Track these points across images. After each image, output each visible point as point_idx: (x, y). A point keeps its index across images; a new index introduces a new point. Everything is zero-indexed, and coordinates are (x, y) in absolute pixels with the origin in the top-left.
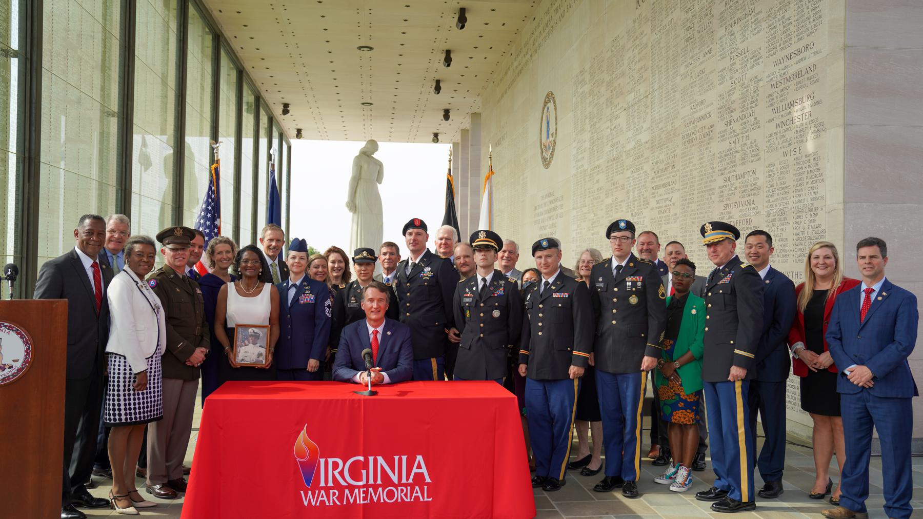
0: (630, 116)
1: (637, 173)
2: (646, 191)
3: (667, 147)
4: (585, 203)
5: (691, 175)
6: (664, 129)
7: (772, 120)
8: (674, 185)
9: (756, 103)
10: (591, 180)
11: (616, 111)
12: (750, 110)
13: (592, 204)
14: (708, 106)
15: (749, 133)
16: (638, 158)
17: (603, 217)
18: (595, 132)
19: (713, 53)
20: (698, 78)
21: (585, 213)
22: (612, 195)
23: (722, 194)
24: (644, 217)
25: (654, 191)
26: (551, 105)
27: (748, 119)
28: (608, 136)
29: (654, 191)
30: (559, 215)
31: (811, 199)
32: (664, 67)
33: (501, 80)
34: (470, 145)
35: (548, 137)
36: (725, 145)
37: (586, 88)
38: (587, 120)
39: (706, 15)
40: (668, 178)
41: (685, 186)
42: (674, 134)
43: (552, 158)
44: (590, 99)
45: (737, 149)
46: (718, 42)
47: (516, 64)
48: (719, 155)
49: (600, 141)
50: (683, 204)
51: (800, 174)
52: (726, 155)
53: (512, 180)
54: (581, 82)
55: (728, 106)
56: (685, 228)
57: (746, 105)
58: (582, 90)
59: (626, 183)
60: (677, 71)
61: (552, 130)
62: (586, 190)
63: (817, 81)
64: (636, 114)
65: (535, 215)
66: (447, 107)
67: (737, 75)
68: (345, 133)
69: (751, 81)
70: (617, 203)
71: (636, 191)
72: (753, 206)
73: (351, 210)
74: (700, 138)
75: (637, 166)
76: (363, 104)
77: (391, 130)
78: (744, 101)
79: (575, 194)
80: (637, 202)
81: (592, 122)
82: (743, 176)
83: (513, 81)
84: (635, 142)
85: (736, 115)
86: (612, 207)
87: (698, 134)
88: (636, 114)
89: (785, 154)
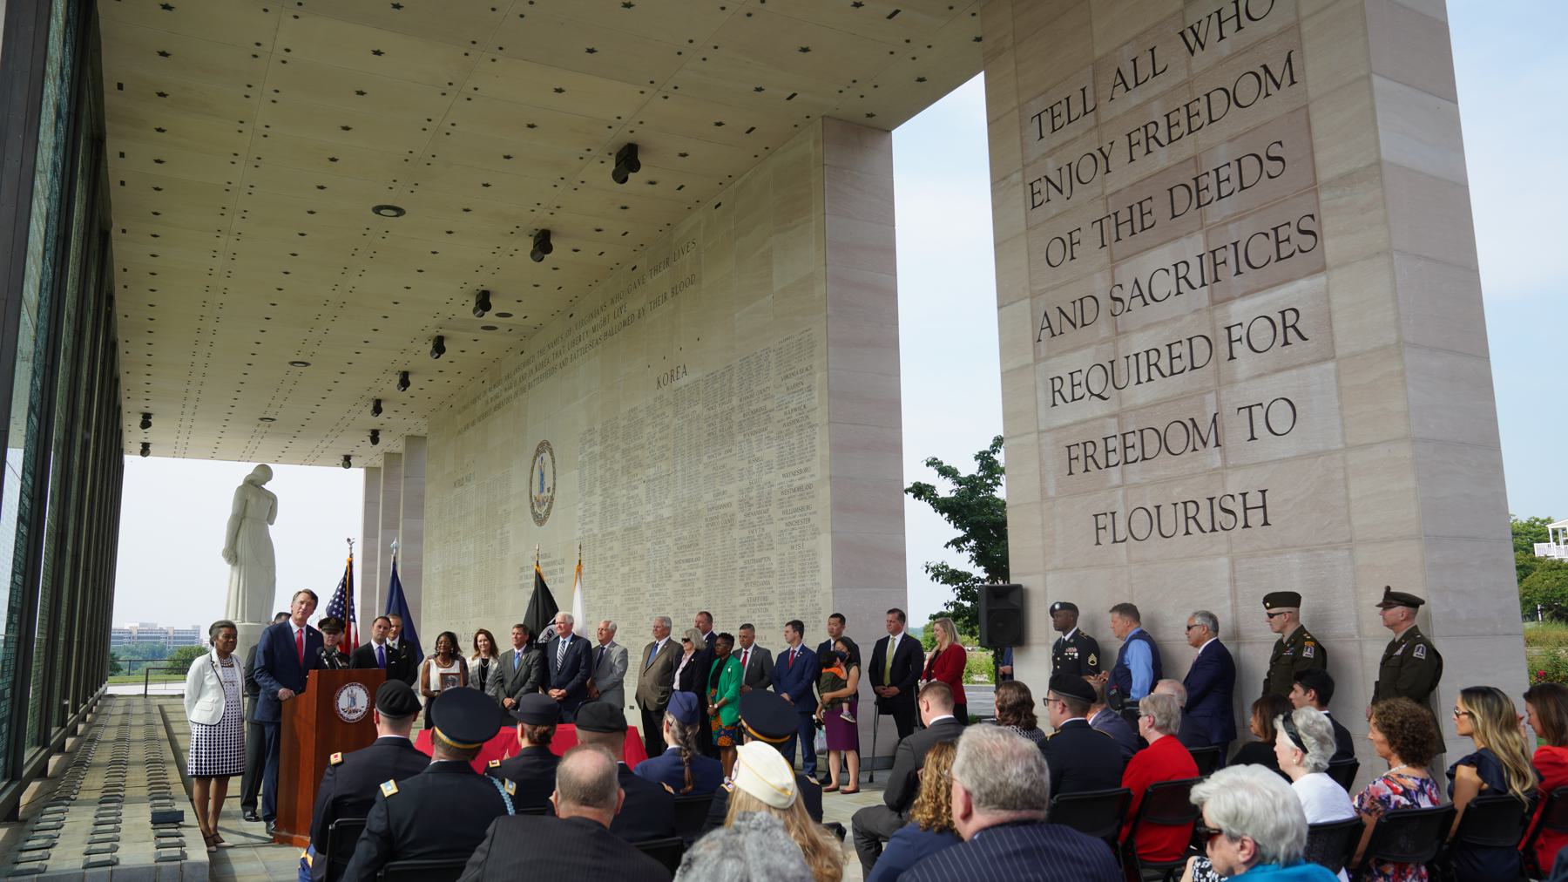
7: (782, 519)
12: (765, 508)
14: (729, 497)
16: (660, 531)
18: (608, 497)
19: (733, 452)
21: (596, 580)
26: (546, 456)
31: (812, 584)
33: (465, 408)
34: (403, 476)
35: (542, 491)
36: (745, 533)
37: (597, 449)
38: (598, 484)
39: (727, 418)
44: (602, 462)
47: (490, 395)
51: (803, 564)
53: (484, 533)
54: (589, 441)
58: (592, 449)
61: (548, 483)
63: (813, 496)
65: (521, 577)
66: (377, 427)
67: (754, 477)
68: (215, 450)
76: (262, 419)
82: (760, 560)
83: (485, 415)
85: (754, 509)
87: (720, 520)
88: (657, 489)
89: (792, 548)
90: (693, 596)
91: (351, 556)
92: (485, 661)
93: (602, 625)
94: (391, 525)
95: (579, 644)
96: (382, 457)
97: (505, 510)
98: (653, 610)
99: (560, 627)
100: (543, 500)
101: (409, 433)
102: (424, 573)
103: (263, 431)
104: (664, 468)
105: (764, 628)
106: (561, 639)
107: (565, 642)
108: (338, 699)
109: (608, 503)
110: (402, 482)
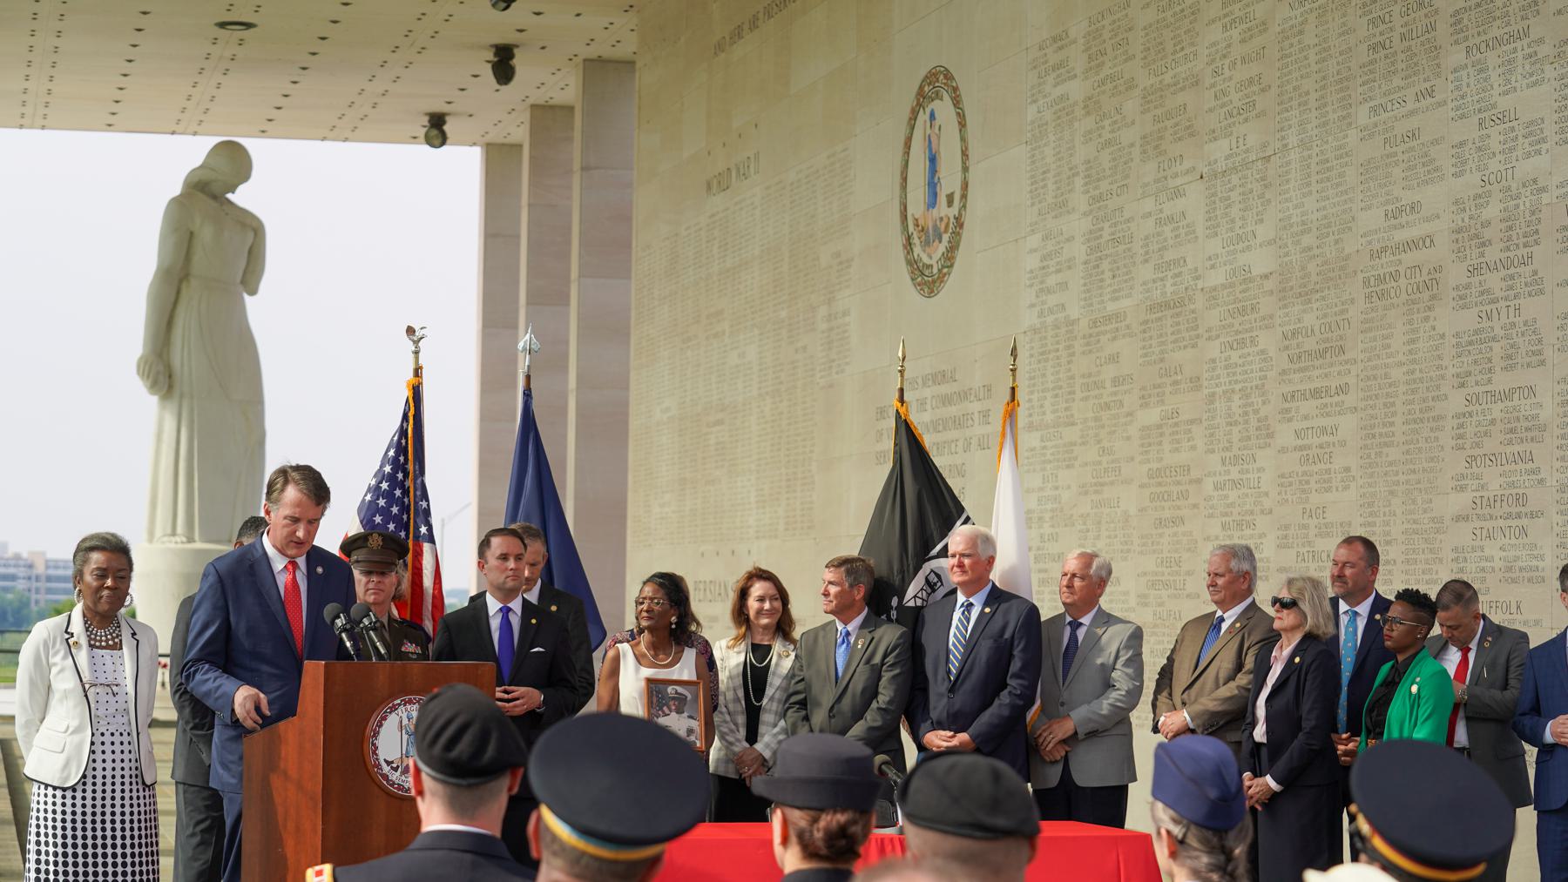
0: (1217, 199)
1: (1240, 352)
2: (1264, 403)
3: (1323, 298)
4: (1072, 416)
5: (1386, 376)
6: (1316, 252)
8: (1343, 397)
9: (1535, 237)
10: (1090, 351)
11: (1176, 175)
12: (1524, 251)
13: (1096, 419)
14: (1427, 220)
15: (1522, 301)
16: (1242, 312)
17: (1133, 459)
19: (1439, 97)
20: (1403, 147)
21: (1073, 444)
22: (1163, 401)
23: (1462, 431)
24: (1261, 470)
25: (1287, 405)
26: (944, 108)
27: (1518, 270)
28: (1147, 238)
29: (1287, 405)
30: (974, 442)
32: (1314, 96)
34: (577, 165)
36: (1468, 320)
37: (1077, 89)
38: (1079, 182)
40: (1326, 376)
41: (1371, 402)
42: (1342, 268)
43: (952, 266)
45: (1496, 332)
46: (1451, 77)
48: (1454, 341)
49: (1121, 248)
50: (1366, 446)
52: (1470, 343)
53: (784, 314)
55: (1473, 231)
56: (1371, 505)
57: (1514, 237)
59: (1206, 375)
60: (1349, 115)
61: (949, 181)
62: (1072, 377)
64: (1234, 196)
67: (1494, 165)
69: (1524, 186)
70: (1176, 424)
71: (1236, 397)
72: (1530, 465)
73: (154, 386)
74: (1410, 291)
75: (1238, 332)
76: (222, 25)
77: (282, 102)
78: (1511, 228)
79: (1034, 385)
80: (1240, 427)
81: (1096, 188)
82: (1507, 395)
84: (1234, 271)
85: (1493, 254)
86: (1162, 435)
87: (1403, 282)
88: (1234, 196)
90: (1328, 490)
91: (418, 372)
92: (761, 651)
93: (1072, 565)
94: (549, 295)
95: (1006, 613)
96: (526, 116)
97: (838, 254)
98: (1223, 527)
99: (961, 565)
100: (936, 228)
101: (593, 52)
102: (635, 423)
103: (228, 54)
104: (1252, 141)
105: (1514, 581)
106: (961, 598)
107: (971, 605)
108: (376, 734)
109: (1106, 237)
110: (576, 180)
